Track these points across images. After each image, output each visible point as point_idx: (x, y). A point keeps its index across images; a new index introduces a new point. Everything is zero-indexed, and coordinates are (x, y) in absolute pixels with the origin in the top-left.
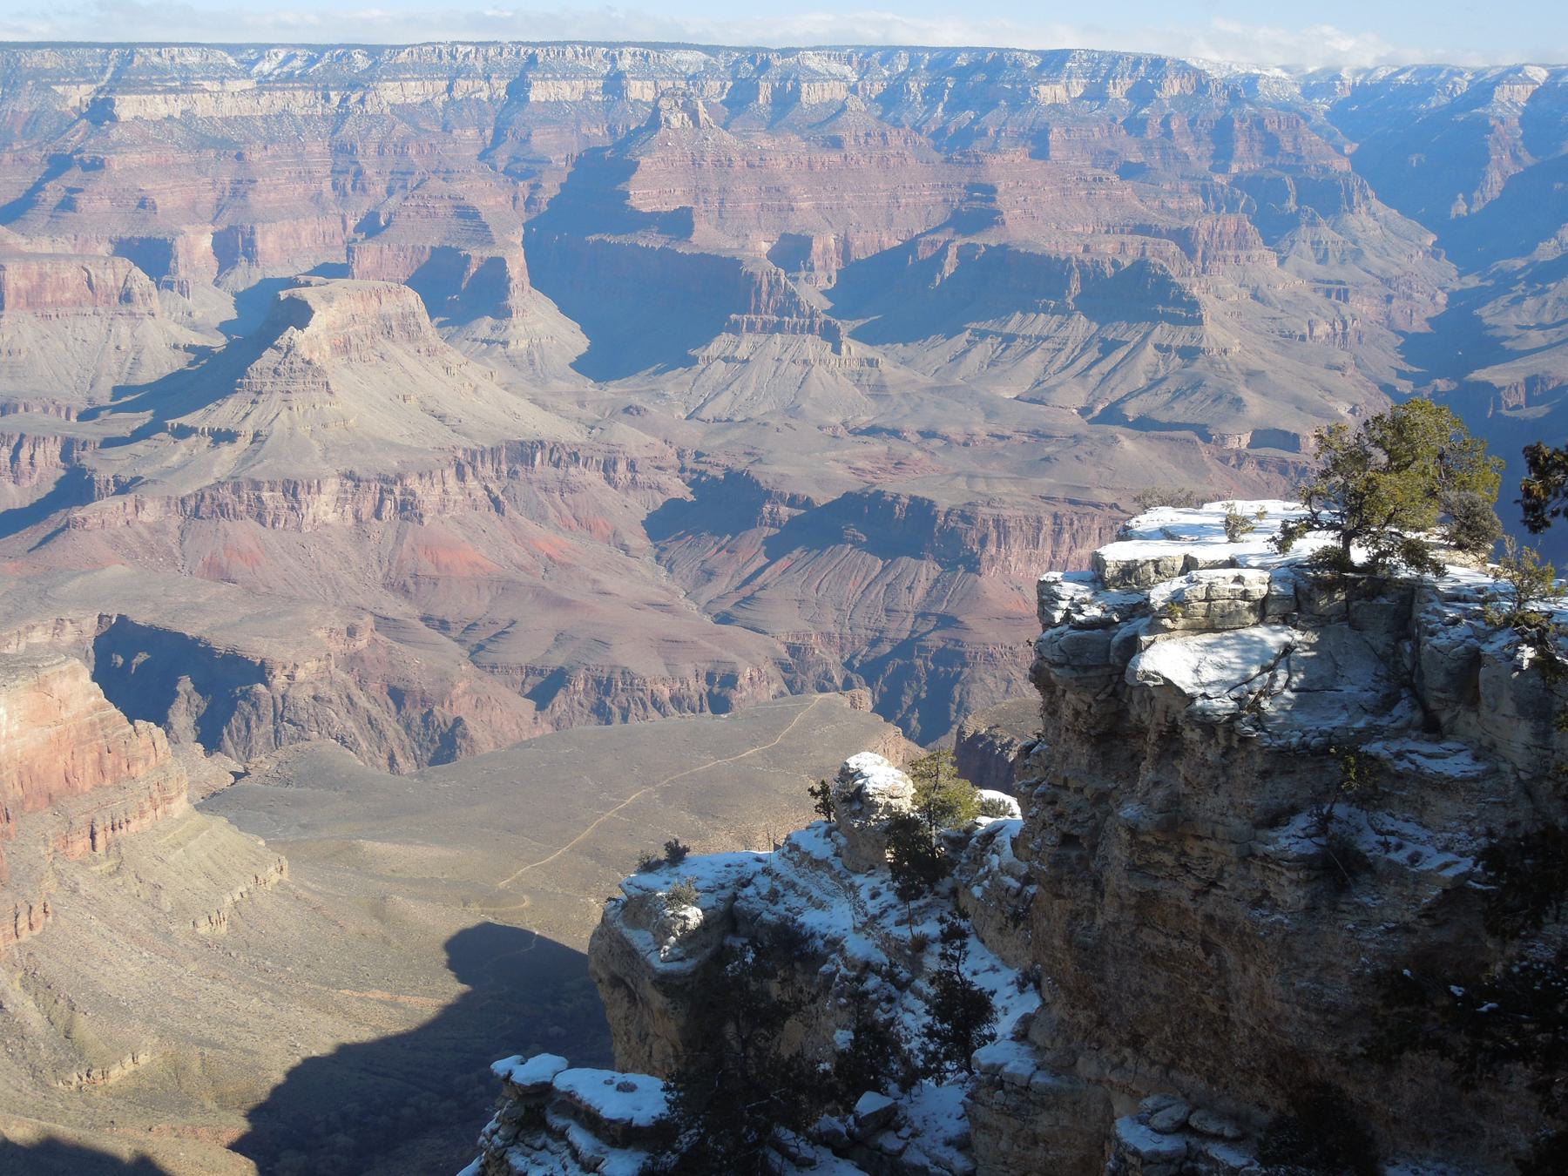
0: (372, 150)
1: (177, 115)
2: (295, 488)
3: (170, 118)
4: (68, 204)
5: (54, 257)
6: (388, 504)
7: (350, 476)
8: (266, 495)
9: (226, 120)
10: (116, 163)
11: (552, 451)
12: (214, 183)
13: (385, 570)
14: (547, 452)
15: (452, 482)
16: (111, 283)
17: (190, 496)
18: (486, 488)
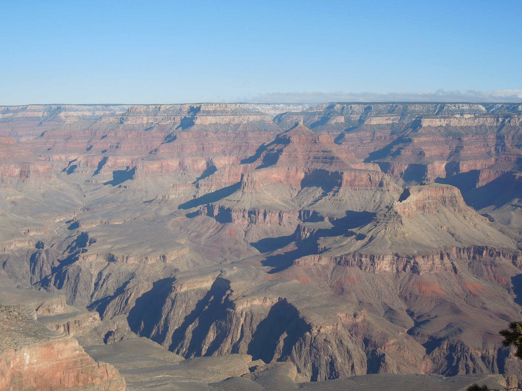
0: (510, 138)
1: (444, 125)
2: (374, 258)
3: (441, 126)
4: (398, 153)
5: (360, 170)
6: (408, 267)
7: (396, 255)
8: (363, 259)
9: (462, 128)
10: (416, 140)
11: (490, 250)
12: (450, 147)
13: (401, 290)
14: (489, 251)
15: (437, 260)
16: (377, 180)
17: (338, 257)
18: (452, 263)
